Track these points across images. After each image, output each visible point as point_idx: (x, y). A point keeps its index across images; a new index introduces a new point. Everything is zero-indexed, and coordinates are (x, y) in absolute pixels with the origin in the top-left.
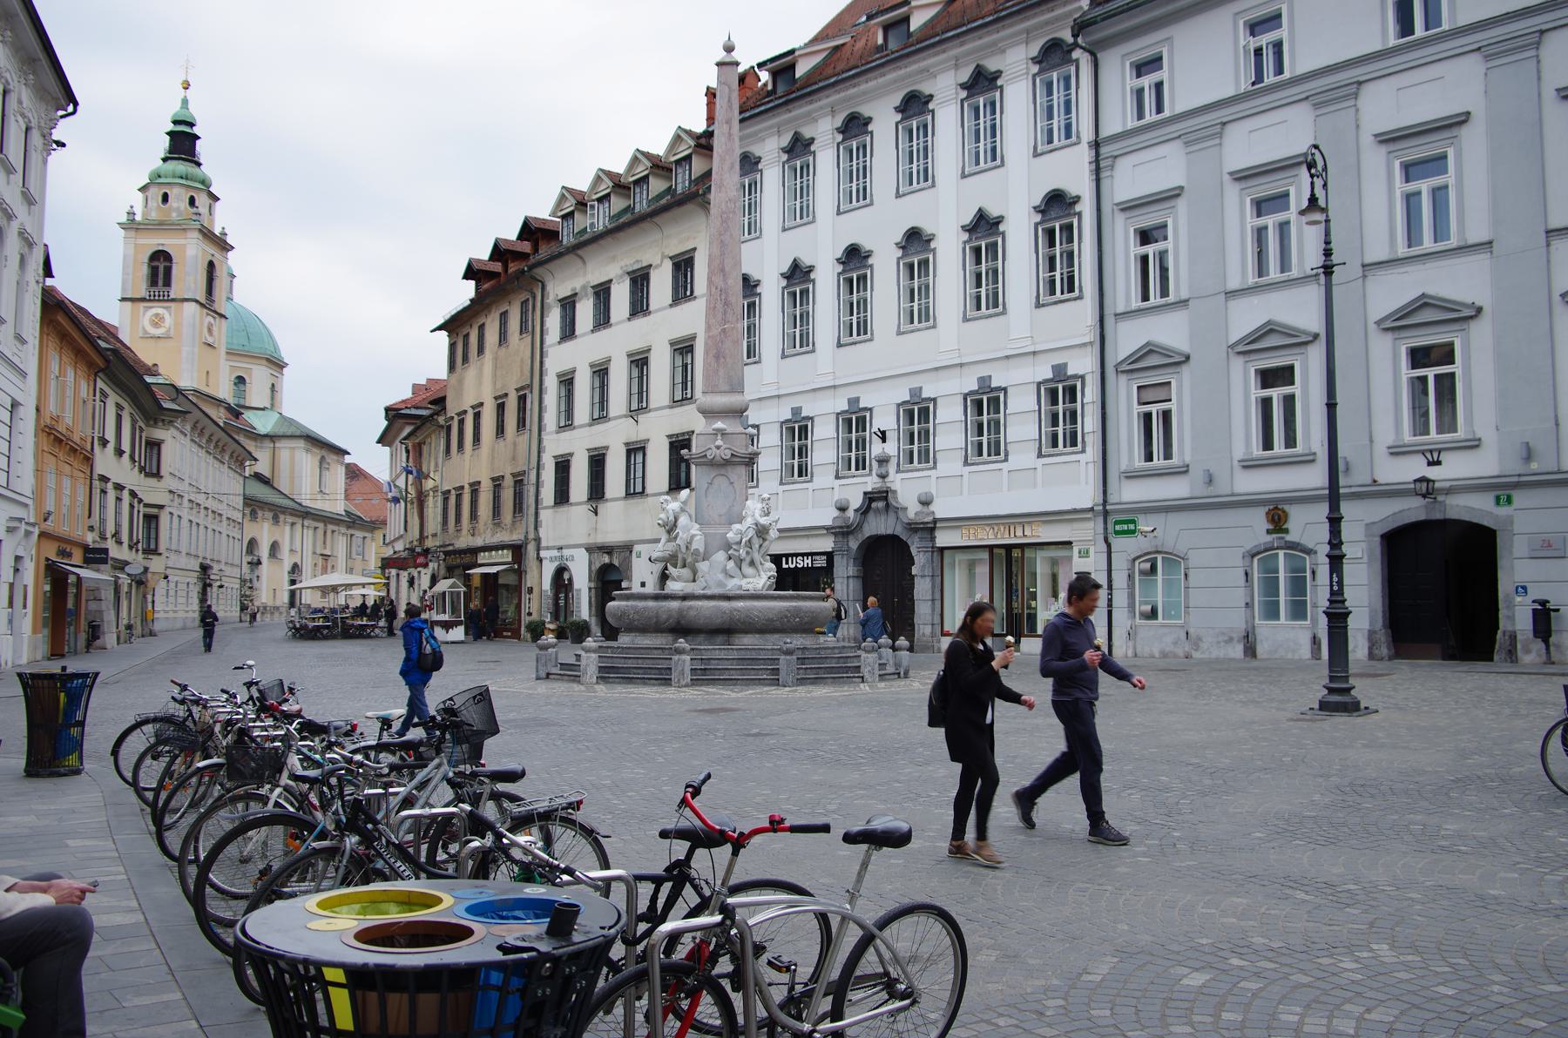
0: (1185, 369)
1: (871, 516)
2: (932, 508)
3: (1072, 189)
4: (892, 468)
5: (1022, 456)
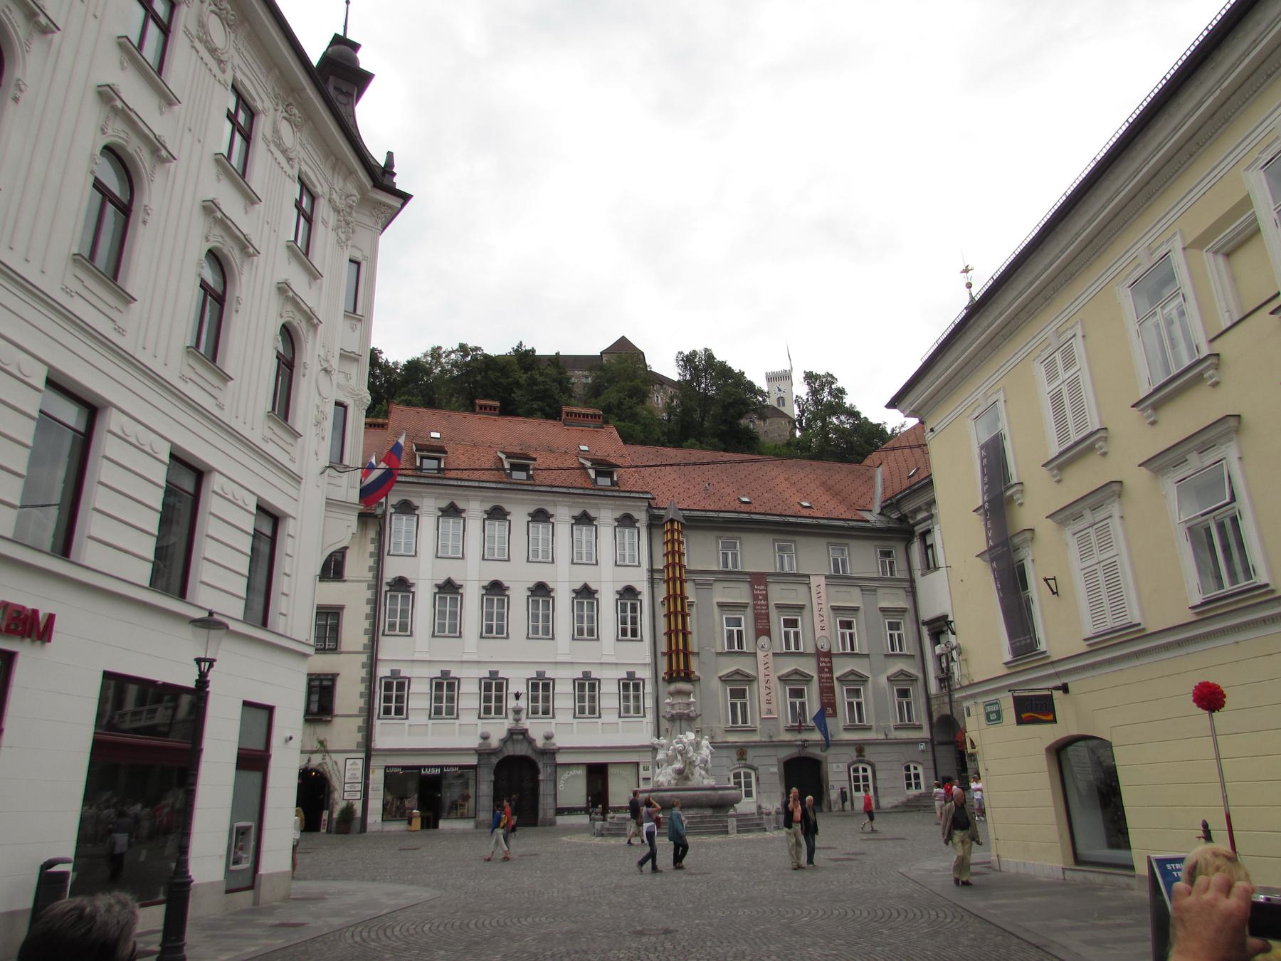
0: (697, 684)
1: (509, 744)
2: (553, 740)
3: (638, 588)
4: (523, 715)
5: (610, 717)
